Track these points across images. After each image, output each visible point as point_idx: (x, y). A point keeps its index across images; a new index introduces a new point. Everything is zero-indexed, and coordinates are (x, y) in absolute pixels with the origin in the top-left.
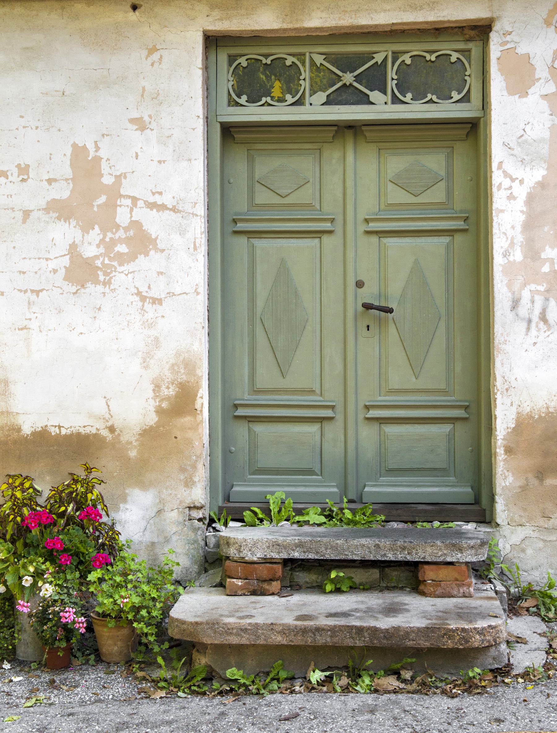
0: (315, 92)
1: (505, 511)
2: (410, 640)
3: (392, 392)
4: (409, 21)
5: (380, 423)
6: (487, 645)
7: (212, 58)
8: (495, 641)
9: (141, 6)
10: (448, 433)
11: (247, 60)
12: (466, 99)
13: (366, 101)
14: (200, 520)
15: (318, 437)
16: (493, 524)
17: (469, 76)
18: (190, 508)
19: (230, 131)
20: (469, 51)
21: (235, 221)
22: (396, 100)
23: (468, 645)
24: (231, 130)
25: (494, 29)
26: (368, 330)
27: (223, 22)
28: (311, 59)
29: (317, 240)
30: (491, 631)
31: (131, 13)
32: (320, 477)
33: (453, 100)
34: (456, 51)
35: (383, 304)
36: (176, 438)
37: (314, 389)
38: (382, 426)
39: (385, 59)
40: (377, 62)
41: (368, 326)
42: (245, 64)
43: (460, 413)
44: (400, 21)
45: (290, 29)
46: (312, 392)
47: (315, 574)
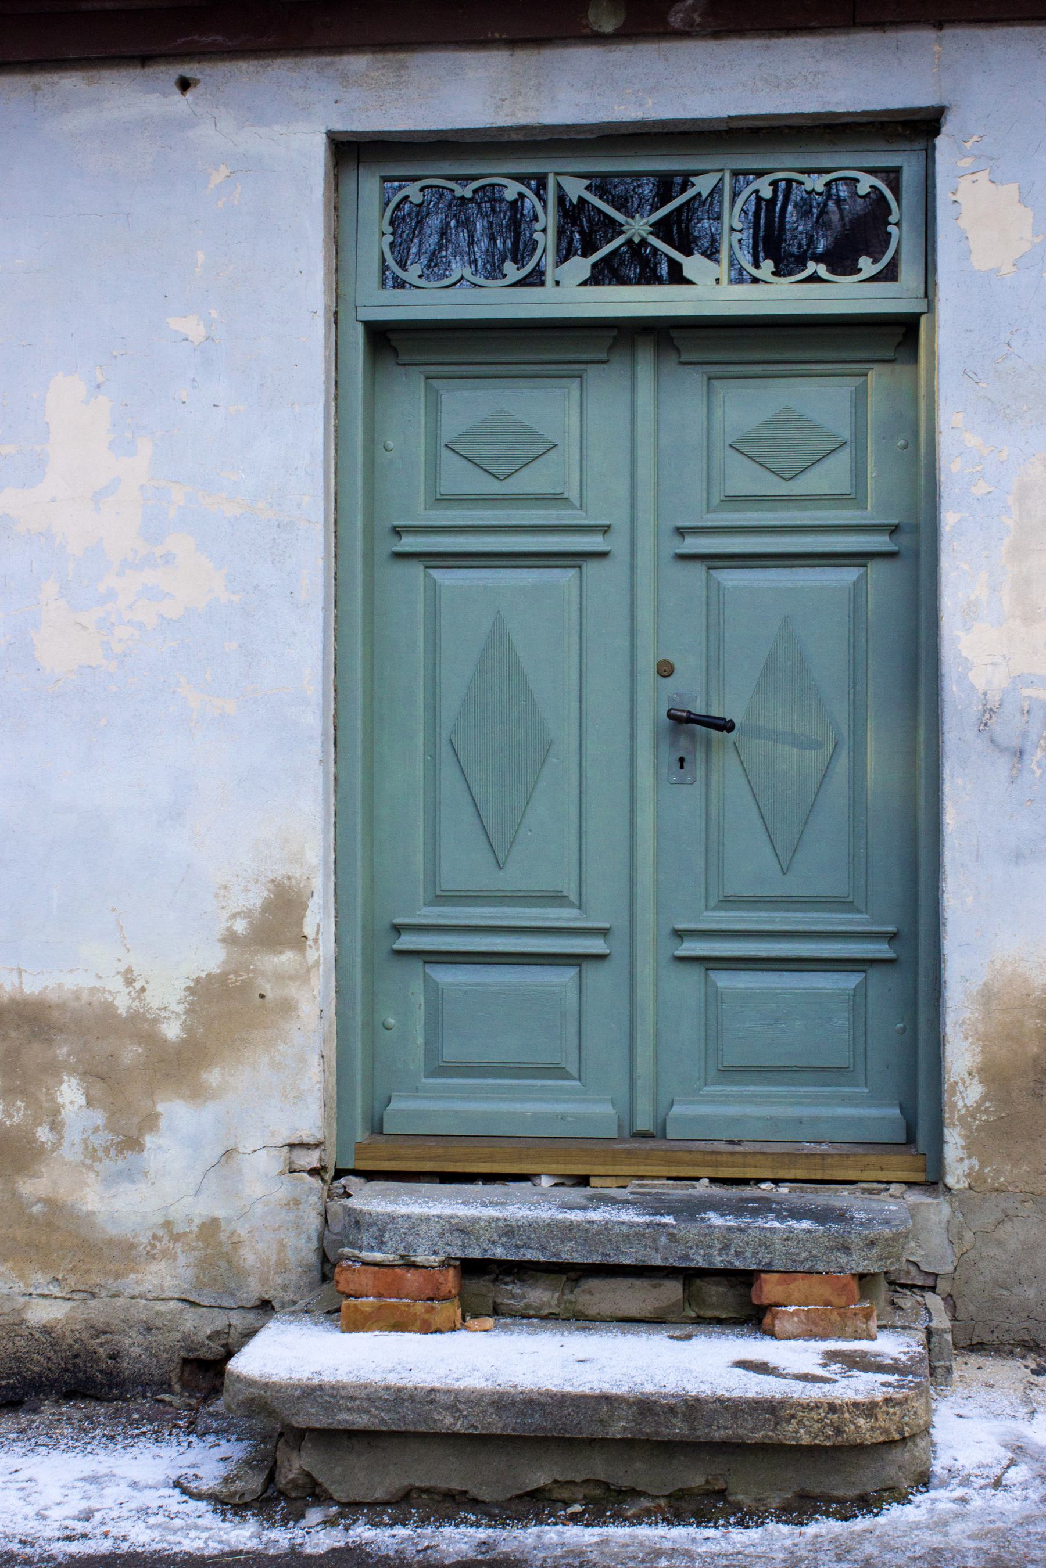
0: (566, 258)
1: (962, 1160)
2: (719, 1428)
3: (731, 902)
4: (764, 112)
5: (707, 969)
6: (882, 1439)
7: (349, 186)
8: (900, 1431)
9: (197, 82)
10: (852, 992)
11: (422, 189)
12: (890, 274)
13: (677, 276)
14: (314, 1172)
15: (572, 996)
16: (941, 1186)
17: (897, 224)
18: (292, 1146)
19: (389, 340)
20: (897, 170)
21: (398, 532)
22: (740, 277)
23: (840, 1439)
24: (390, 335)
25: (944, 129)
26: (682, 767)
27: (370, 113)
28: (559, 186)
29: (572, 572)
30: (891, 1410)
31: (177, 96)
32: (577, 1083)
33: (862, 276)
34: (871, 171)
35: (715, 712)
36: (262, 996)
37: (565, 893)
38: (710, 973)
39: (717, 190)
40: (699, 194)
41: (682, 760)
42: (417, 198)
43: (881, 950)
44: (322, 481)
45: (511, 127)
46: (557, 898)
47: (546, 1290)
